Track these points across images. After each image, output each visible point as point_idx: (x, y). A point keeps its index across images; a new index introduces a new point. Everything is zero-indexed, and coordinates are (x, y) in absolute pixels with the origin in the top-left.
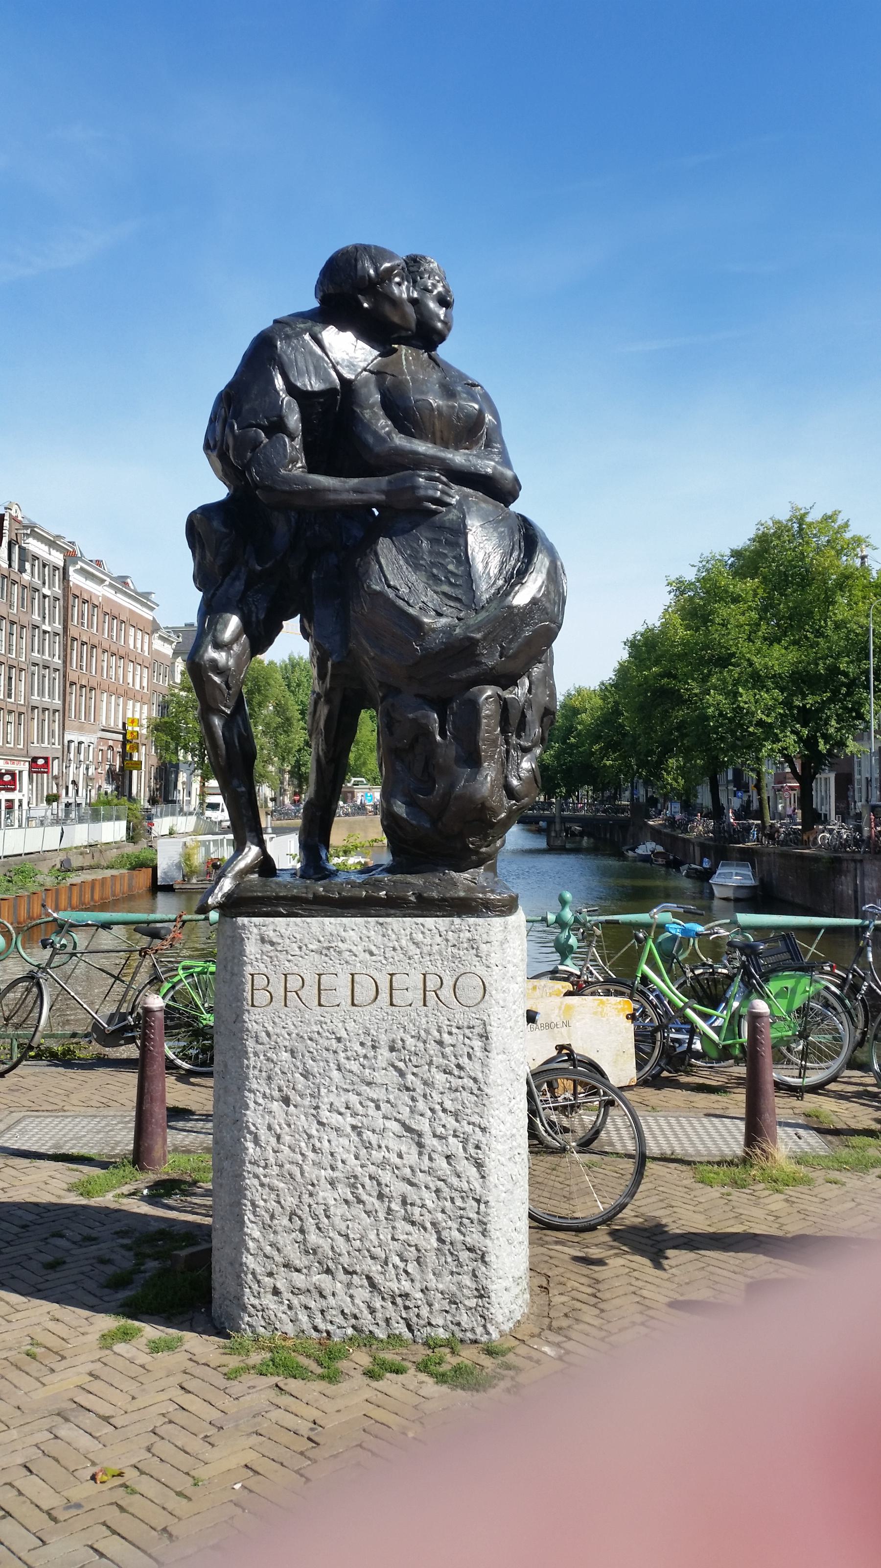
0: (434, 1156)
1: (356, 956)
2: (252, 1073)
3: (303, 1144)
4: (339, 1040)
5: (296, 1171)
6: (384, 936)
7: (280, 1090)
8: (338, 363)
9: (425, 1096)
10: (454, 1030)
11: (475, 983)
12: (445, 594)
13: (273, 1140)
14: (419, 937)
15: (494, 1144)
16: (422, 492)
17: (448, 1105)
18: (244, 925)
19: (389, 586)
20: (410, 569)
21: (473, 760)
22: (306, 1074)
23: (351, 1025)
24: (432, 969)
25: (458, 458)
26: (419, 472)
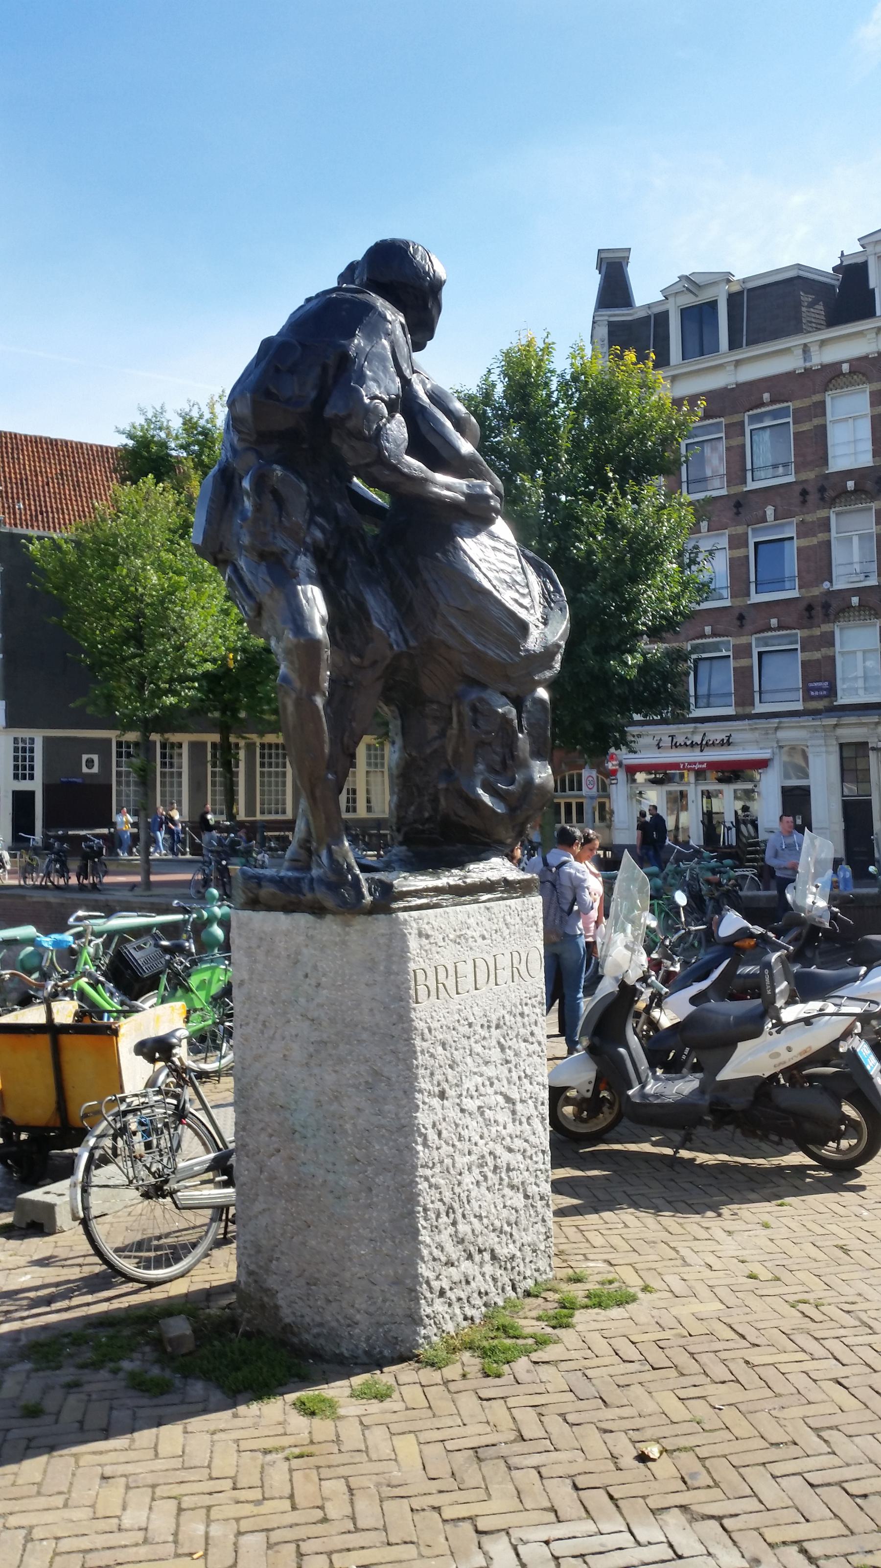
2: (421, 1071)
18: (406, 920)
23: (476, 1009)
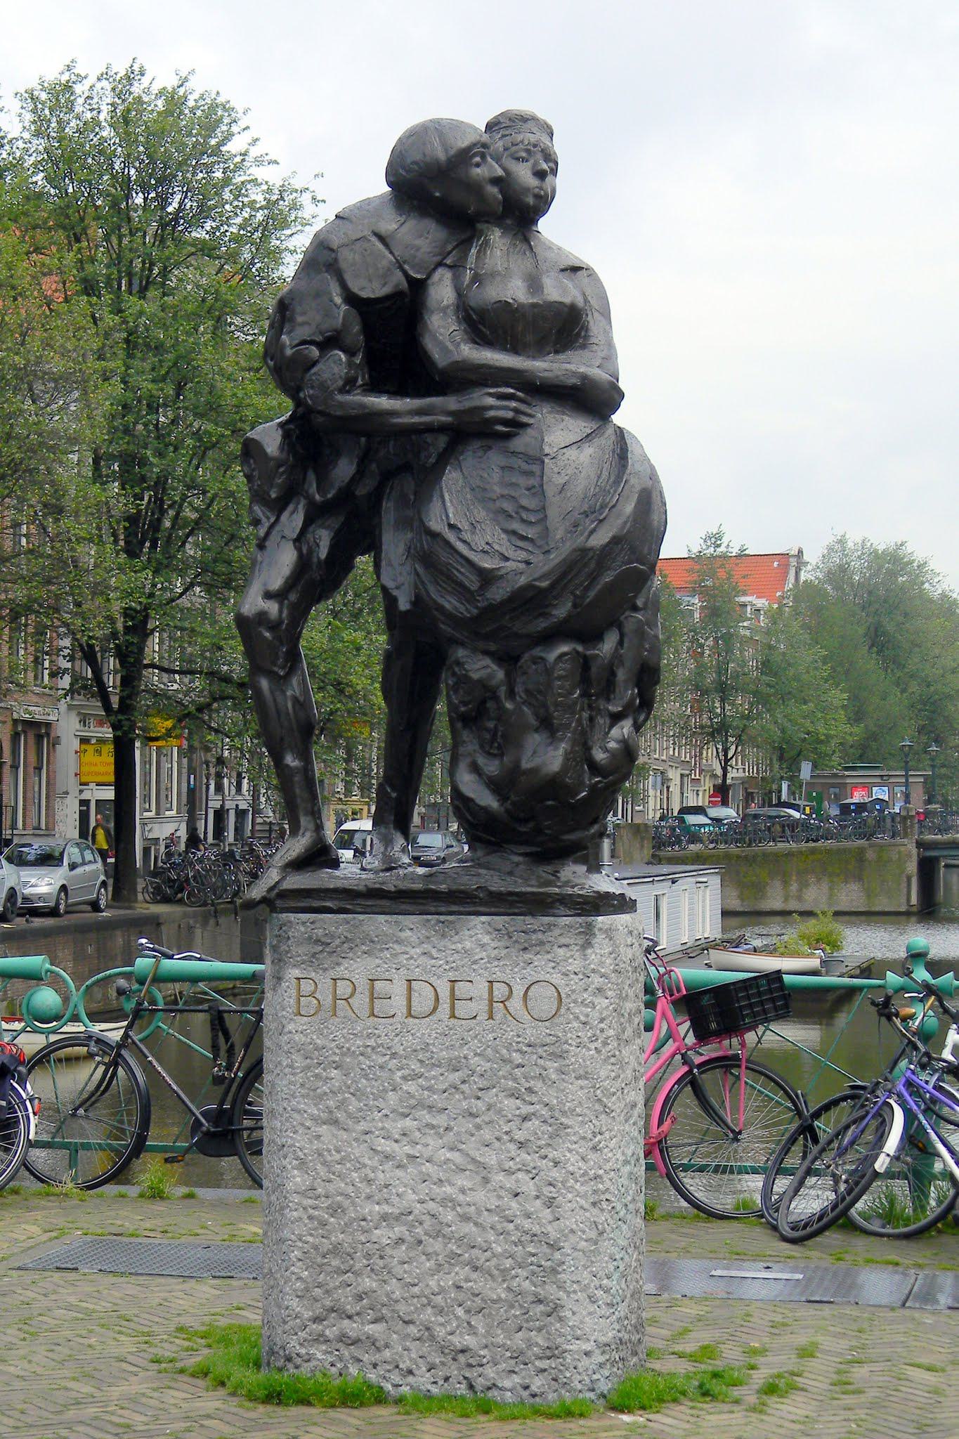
5: (346, 1203)
12: (514, 533)
16: (492, 413)
24: (499, 975)
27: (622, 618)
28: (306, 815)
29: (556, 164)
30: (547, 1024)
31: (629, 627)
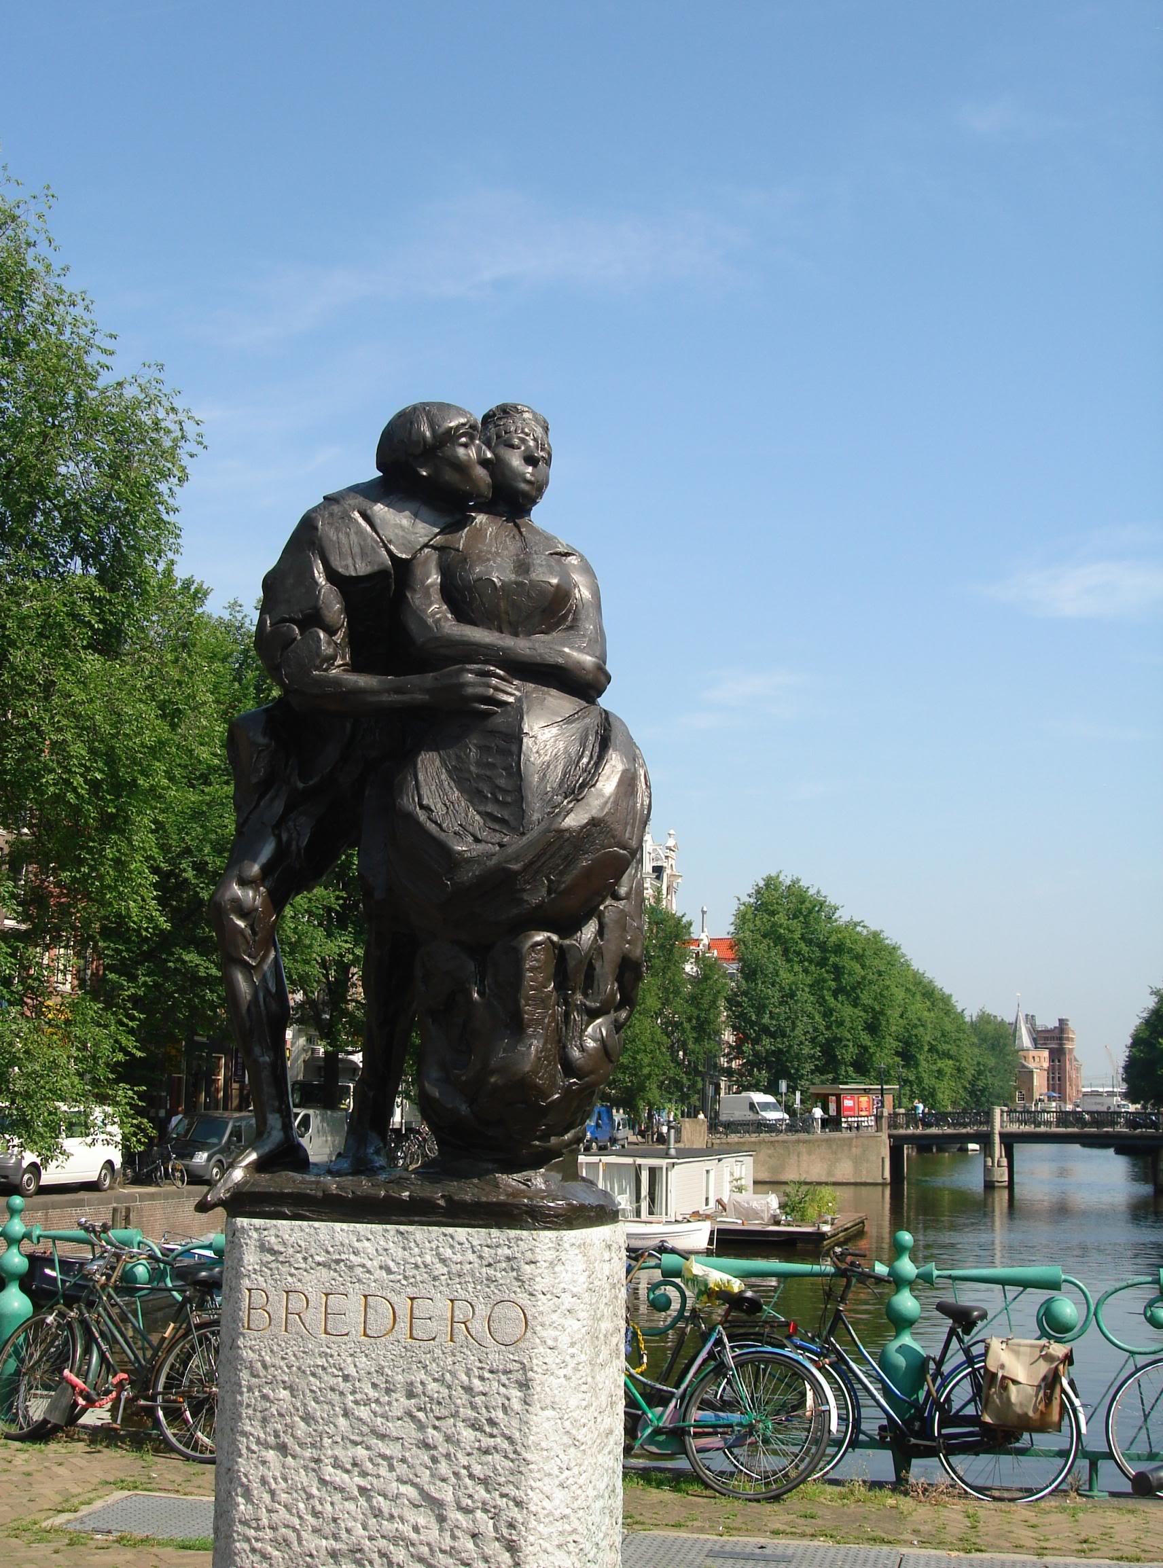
0: (458, 1533)
1: (369, 1272)
2: (245, 1412)
3: (301, 1506)
4: (346, 1378)
5: (292, 1536)
6: (404, 1249)
7: (277, 1436)
8: (390, 542)
9: (448, 1456)
10: (487, 1375)
11: (513, 1315)
13: (267, 1497)
14: (448, 1253)
15: (533, 1523)
16: (470, 690)
17: (477, 1470)
19: (422, 807)
20: (452, 784)
21: (517, 1027)
22: (308, 1418)
24: (462, 1294)
25: (523, 646)
26: (468, 667)
27: (602, 908)
28: (273, 1111)
29: (550, 455)
30: (511, 1348)
31: (609, 917)
